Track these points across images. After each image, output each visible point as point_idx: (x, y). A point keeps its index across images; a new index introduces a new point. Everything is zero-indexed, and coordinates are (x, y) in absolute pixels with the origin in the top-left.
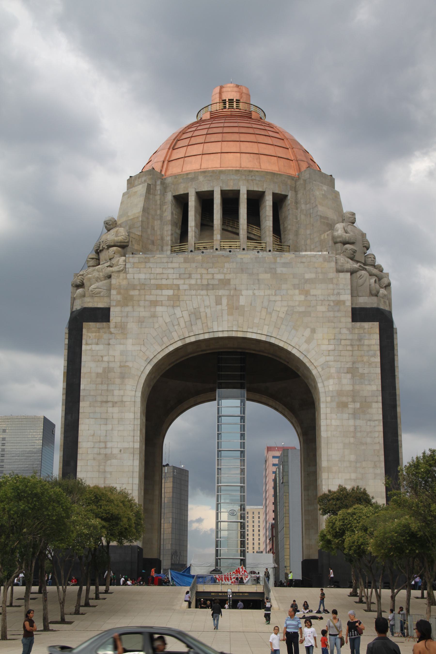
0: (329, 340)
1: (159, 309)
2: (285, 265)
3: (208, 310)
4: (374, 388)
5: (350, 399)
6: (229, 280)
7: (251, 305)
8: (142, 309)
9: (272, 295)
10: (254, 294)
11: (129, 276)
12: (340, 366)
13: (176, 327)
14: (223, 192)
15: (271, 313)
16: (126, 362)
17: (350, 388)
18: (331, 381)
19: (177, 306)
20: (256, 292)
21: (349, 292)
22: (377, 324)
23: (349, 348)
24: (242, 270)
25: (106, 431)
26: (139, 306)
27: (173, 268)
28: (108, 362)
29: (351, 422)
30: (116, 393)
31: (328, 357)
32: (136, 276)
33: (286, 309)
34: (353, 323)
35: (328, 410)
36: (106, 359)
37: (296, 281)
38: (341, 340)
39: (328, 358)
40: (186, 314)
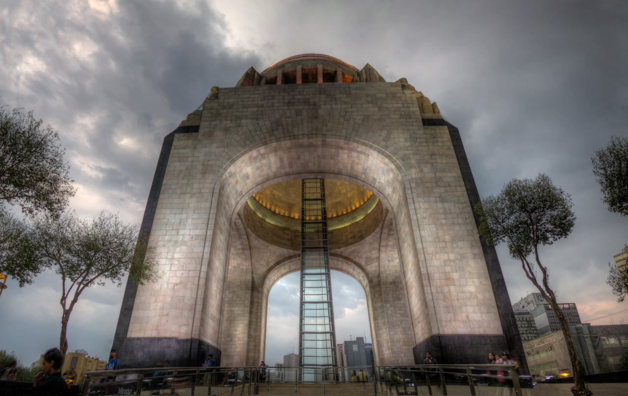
0: (406, 139)
1: (244, 121)
2: (357, 89)
3: (289, 120)
4: (455, 174)
5: (434, 185)
6: (309, 99)
7: (329, 115)
8: (229, 122)
9: (348, 108)
10: (332, 108)
11: (220, 101)
12: (419, 158)
13: (258, 133)
14: (303, 69)
15: (348, 120)
16: (209, 161)
17: (431, 175)
18: (413, 171)
19: (261, 119)
20: (334, 106)
21: (417, 105)
22: (446, 127)
23: (424, 144)
24: (320, 93)
25: (181, 219)
26: (227, 120)
27: (259, 94)
28: (192, 162)
29: (440, 205)
30: (195, 186)
31: (407, 152)
32: (226, 101)
33: (362, 117)
34: (425, 126)
35: (415, 195)
36: (190, 159)
37: (369, 99)
38: (417, 138)
39: (407, 152)
40: (268, 123)
